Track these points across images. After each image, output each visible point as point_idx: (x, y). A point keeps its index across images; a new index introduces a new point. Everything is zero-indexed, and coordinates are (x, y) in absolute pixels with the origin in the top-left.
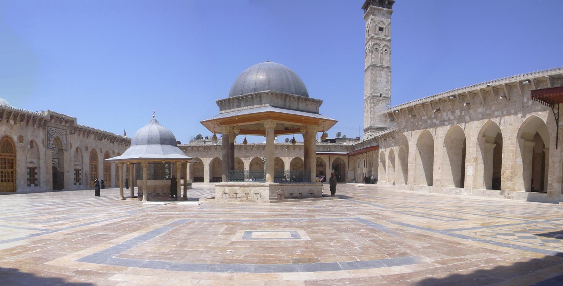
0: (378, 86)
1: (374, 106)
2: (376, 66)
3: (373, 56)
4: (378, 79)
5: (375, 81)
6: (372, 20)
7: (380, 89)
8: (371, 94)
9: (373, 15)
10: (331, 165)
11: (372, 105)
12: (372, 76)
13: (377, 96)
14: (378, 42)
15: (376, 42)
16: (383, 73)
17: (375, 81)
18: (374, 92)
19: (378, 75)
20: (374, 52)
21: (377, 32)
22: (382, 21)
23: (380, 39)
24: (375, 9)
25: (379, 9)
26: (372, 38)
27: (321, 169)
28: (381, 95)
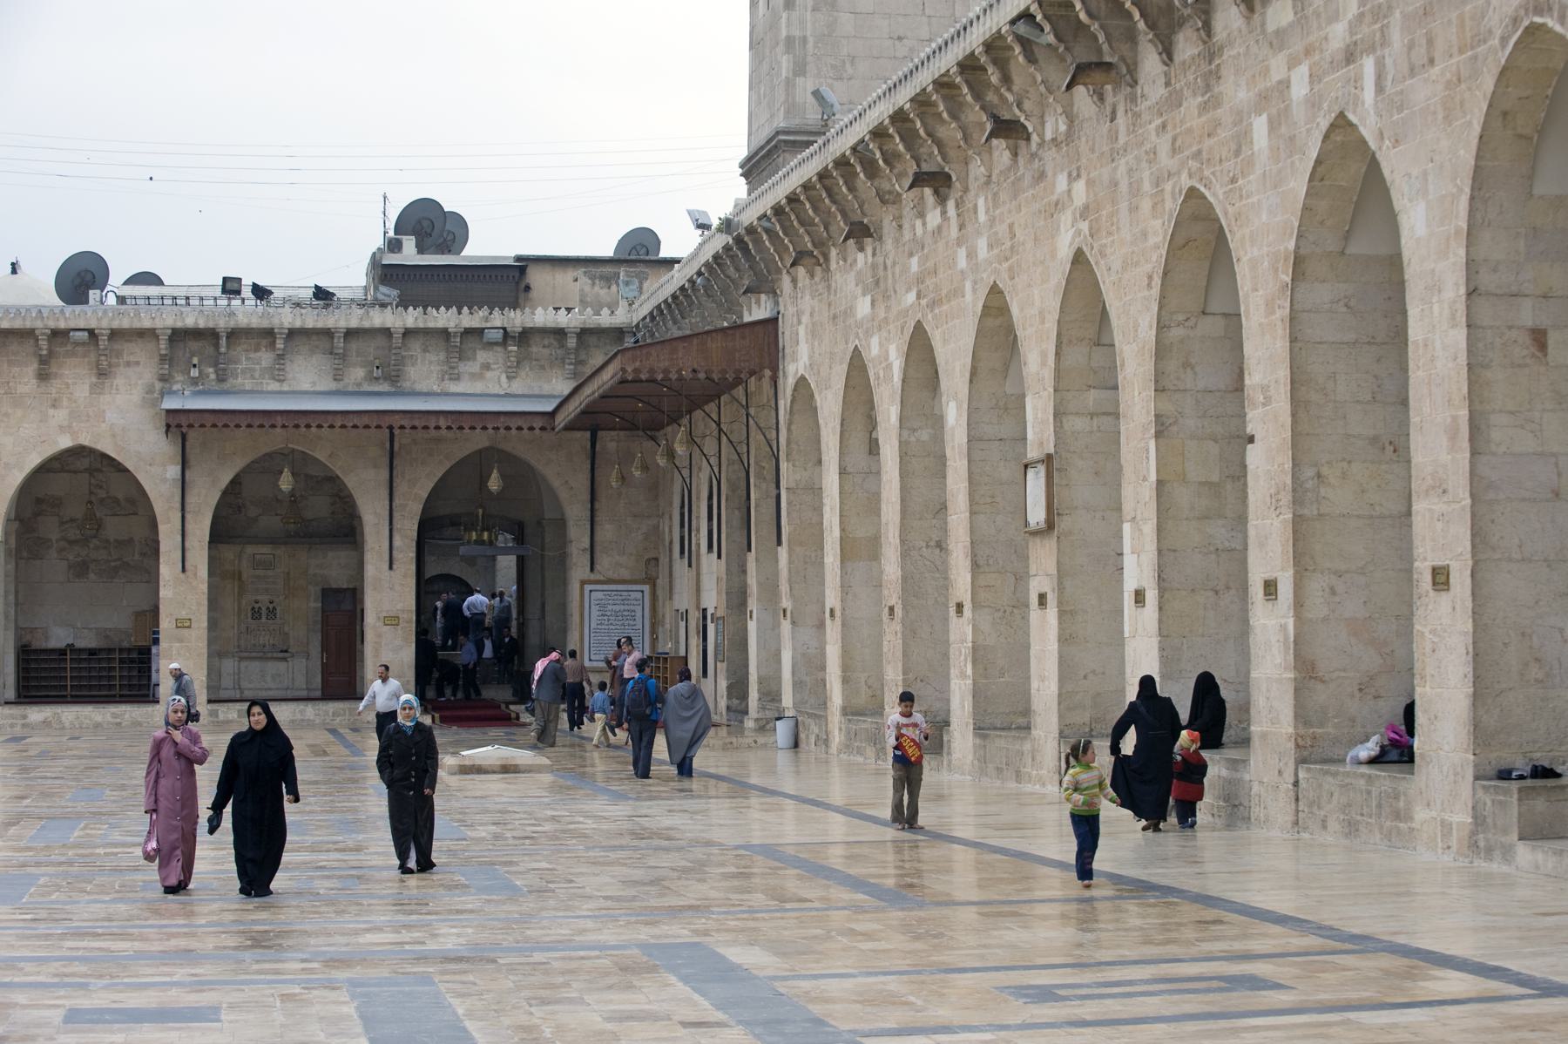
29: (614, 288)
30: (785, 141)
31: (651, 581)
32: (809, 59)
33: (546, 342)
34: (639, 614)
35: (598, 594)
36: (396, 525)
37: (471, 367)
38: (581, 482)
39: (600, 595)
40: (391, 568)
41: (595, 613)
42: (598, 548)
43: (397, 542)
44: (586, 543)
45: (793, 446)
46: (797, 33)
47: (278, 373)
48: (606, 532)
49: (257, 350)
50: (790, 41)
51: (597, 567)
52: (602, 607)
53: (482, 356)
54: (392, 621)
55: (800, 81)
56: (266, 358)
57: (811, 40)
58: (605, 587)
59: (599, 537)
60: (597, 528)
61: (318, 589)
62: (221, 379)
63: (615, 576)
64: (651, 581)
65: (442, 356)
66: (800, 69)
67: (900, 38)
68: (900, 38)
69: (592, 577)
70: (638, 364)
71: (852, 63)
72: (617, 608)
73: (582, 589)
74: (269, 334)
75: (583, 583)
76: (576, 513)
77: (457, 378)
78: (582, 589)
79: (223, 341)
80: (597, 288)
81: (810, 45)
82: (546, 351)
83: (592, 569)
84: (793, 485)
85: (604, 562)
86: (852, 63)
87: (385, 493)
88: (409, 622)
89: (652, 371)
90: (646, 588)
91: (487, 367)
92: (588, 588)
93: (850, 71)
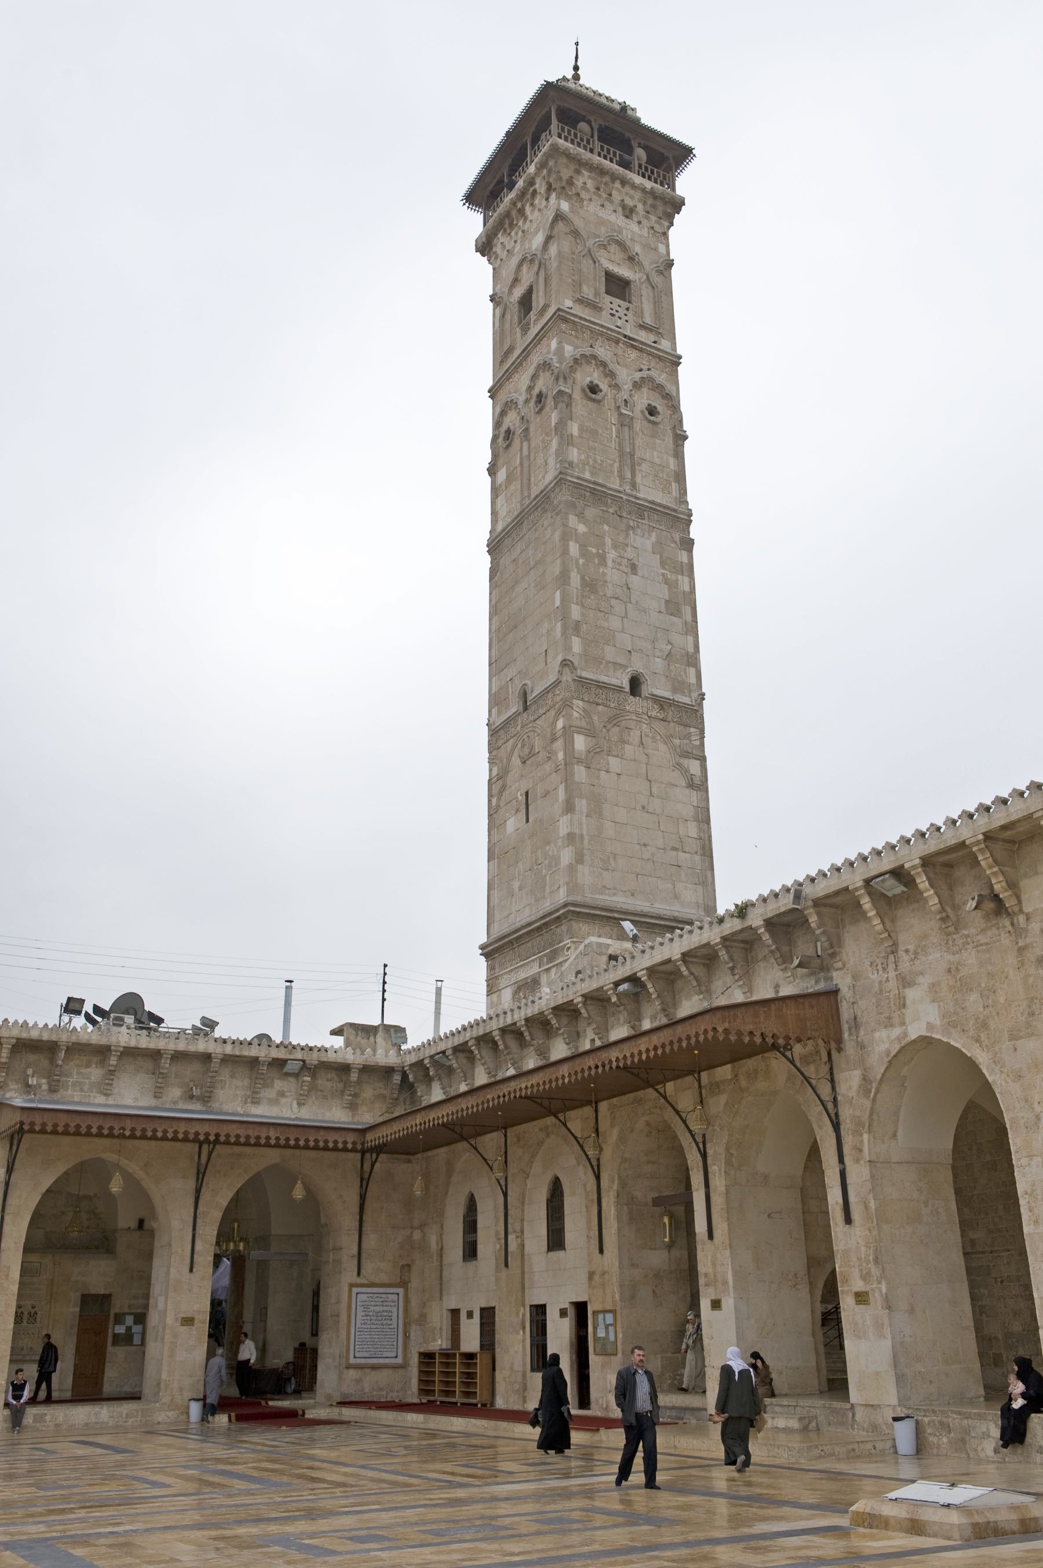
0: (615, 623)
1: (595, 752)
2: (597, 494)
3: (574, 429)
4: (613, 576)
5: (590, 586)
6: (559, 217)
7: (625, 641)
8: (566, 663)
9: (563, 193)
10: (209, 1232)
11: (580, 743)
12: (574, 548)
13: (619, 689)
14: (603, 351)
15: (588, 351)
16: (644, 543)
17: (590, 586)
18: (592, 659)
19: (612, 555)
20: (581, 406)
21: (588, 292)
22: (622, 245)
23: (615, 339)
24: (581, 164)
25: (602, 172)
26: (562, 316)
27: (96, 1274)
28: (635, 684)
29: (372, 1039)
30: (573, 912)
31: (404, 1284)
32: (586, 852)
33: (329, 1076)
34: (395, 1315)
35: (363, 1296)
36: (199, 1231)
37: (269, 1093)
38: (352, 1196)
39: (364, 1297)
40: (191, 1270)
41: (360, 1314)
42: (364, 1255)
43: (199, 1246)
44: (355, 1250)
45: (875, 1117)
46: (577, 831)
47: (105, 1088)
48: (371, 1240)
49: (88, 1066)
50: (571, 838)
51: (363, 1271)
52: (366, 1307)
53: (279, 1084)
54: (188, 1321)
55: (580, 867)
56: (95, 1073)
57: (586, 837)
58: (369, 1290)
59: (364, 1245)
60: (364, 1237)
61: (79, 1294)
62: (52, 1090)
63: (377, 1281)
64: (404, 1284)
65: (246, 1082)
66: (579, 859)
67: (645, 845)
68: (645, 845)
69: (359, 1281)
70: (727, 1025)
71: (615, 858)
72: (378, 1309)
73: (350, 1291)
74: (102, 1052)
75: (352, 1285)
76: (348, 1221)
77: (256, 1102)
78: (350, 1291)
79: (62, 1055)
80: (359, 1038)
81: (586, 842)
82: (329, 1084)
83: (359, 1274)
84: (874, 1158)
85: (368, 1267)
86: (615, 858)
87: (191, 1201)
88: (203, 1322)
89: (739, 1033)
90: (401, 1291)
91: (281, 1094)
92: (355, 1290)
93: (613, 865)
